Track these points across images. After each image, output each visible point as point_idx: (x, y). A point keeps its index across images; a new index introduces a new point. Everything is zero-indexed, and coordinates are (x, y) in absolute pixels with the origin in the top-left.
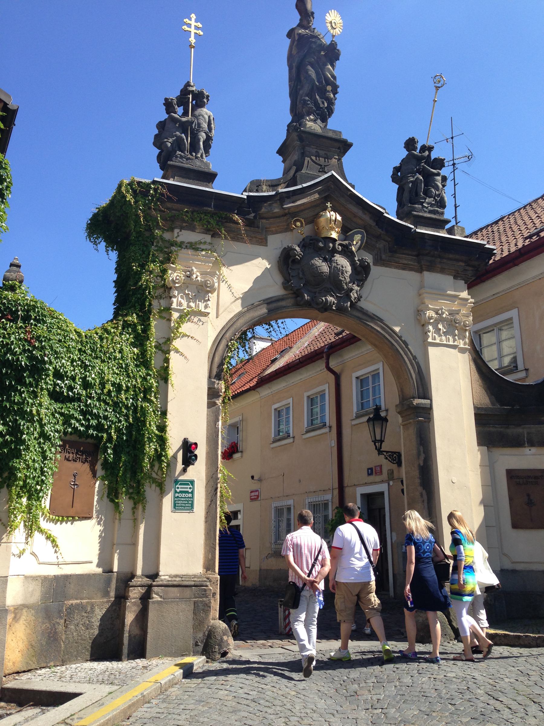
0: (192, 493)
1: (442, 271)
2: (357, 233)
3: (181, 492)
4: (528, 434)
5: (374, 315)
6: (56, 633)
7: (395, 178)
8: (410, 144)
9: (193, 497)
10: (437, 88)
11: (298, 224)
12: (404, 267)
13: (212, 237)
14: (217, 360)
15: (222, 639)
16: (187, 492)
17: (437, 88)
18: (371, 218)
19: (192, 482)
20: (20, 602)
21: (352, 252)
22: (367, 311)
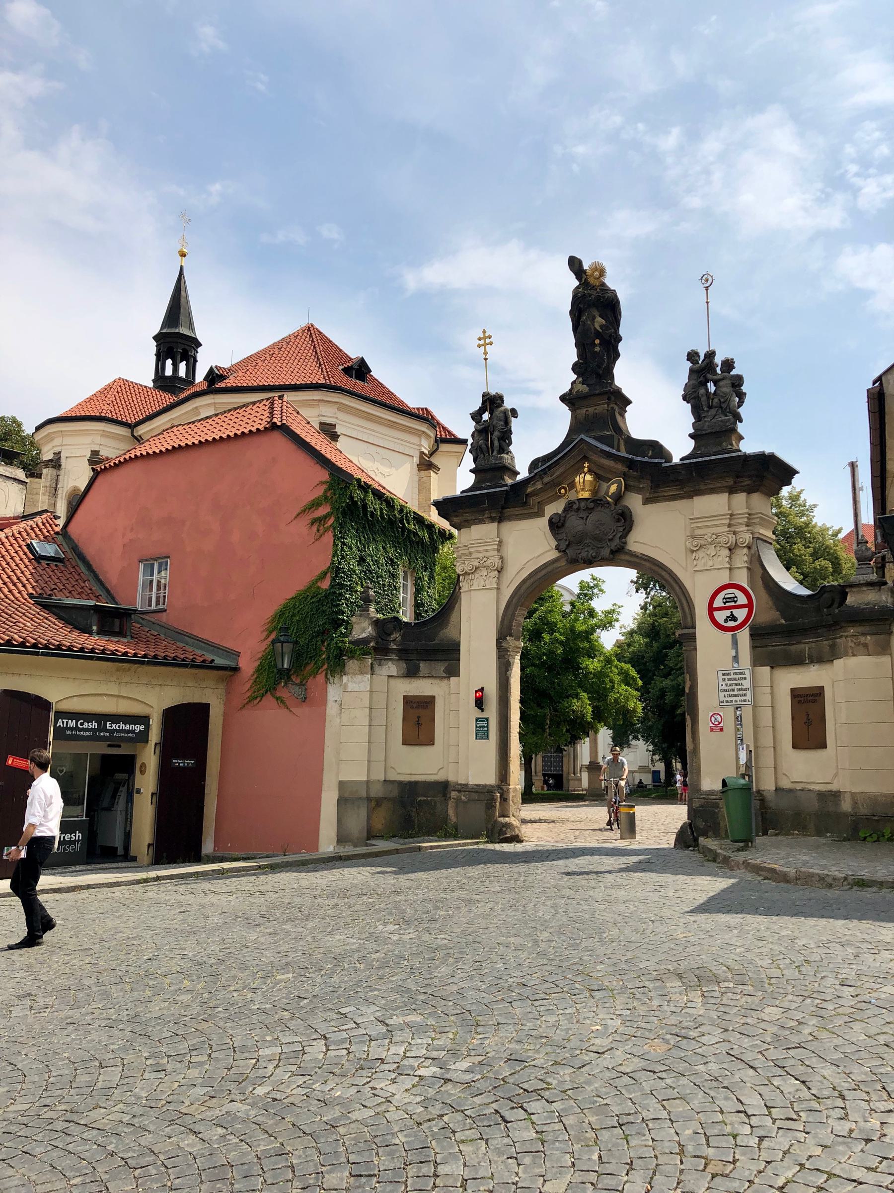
0: (487, 727)
1: (712, 491)
2: (612, 484)
3: (480, 727)
4: (809, 648)
5: (642, 554)
6: (410, 816)
7: (685, 398)
8: (692, 356)
9: (487, 730)
10: (707, 289)
11: (563, 491)
12: (674, 498)
13: (499, 522)
14: (506, 622)
15: (501, 829)
16: (484, 727)
17: (707, 289)
18: (623, 466)
19: (487, 719)
20: (380, 795)
21: (608, 503)
22: (635, 552)
